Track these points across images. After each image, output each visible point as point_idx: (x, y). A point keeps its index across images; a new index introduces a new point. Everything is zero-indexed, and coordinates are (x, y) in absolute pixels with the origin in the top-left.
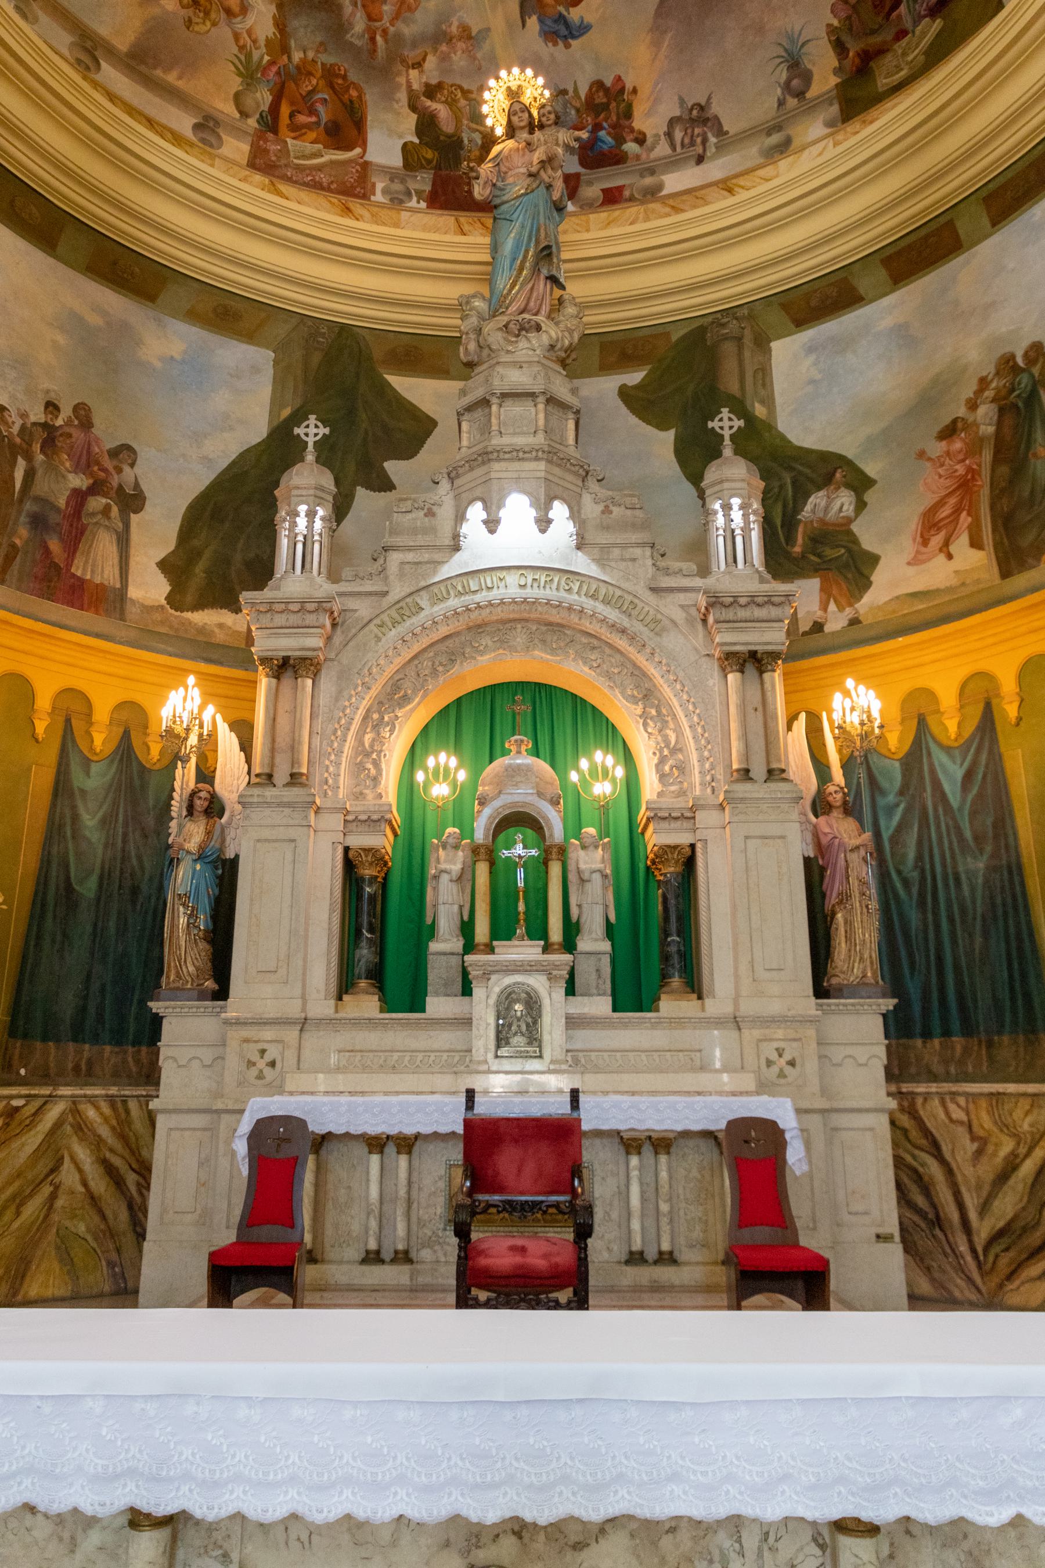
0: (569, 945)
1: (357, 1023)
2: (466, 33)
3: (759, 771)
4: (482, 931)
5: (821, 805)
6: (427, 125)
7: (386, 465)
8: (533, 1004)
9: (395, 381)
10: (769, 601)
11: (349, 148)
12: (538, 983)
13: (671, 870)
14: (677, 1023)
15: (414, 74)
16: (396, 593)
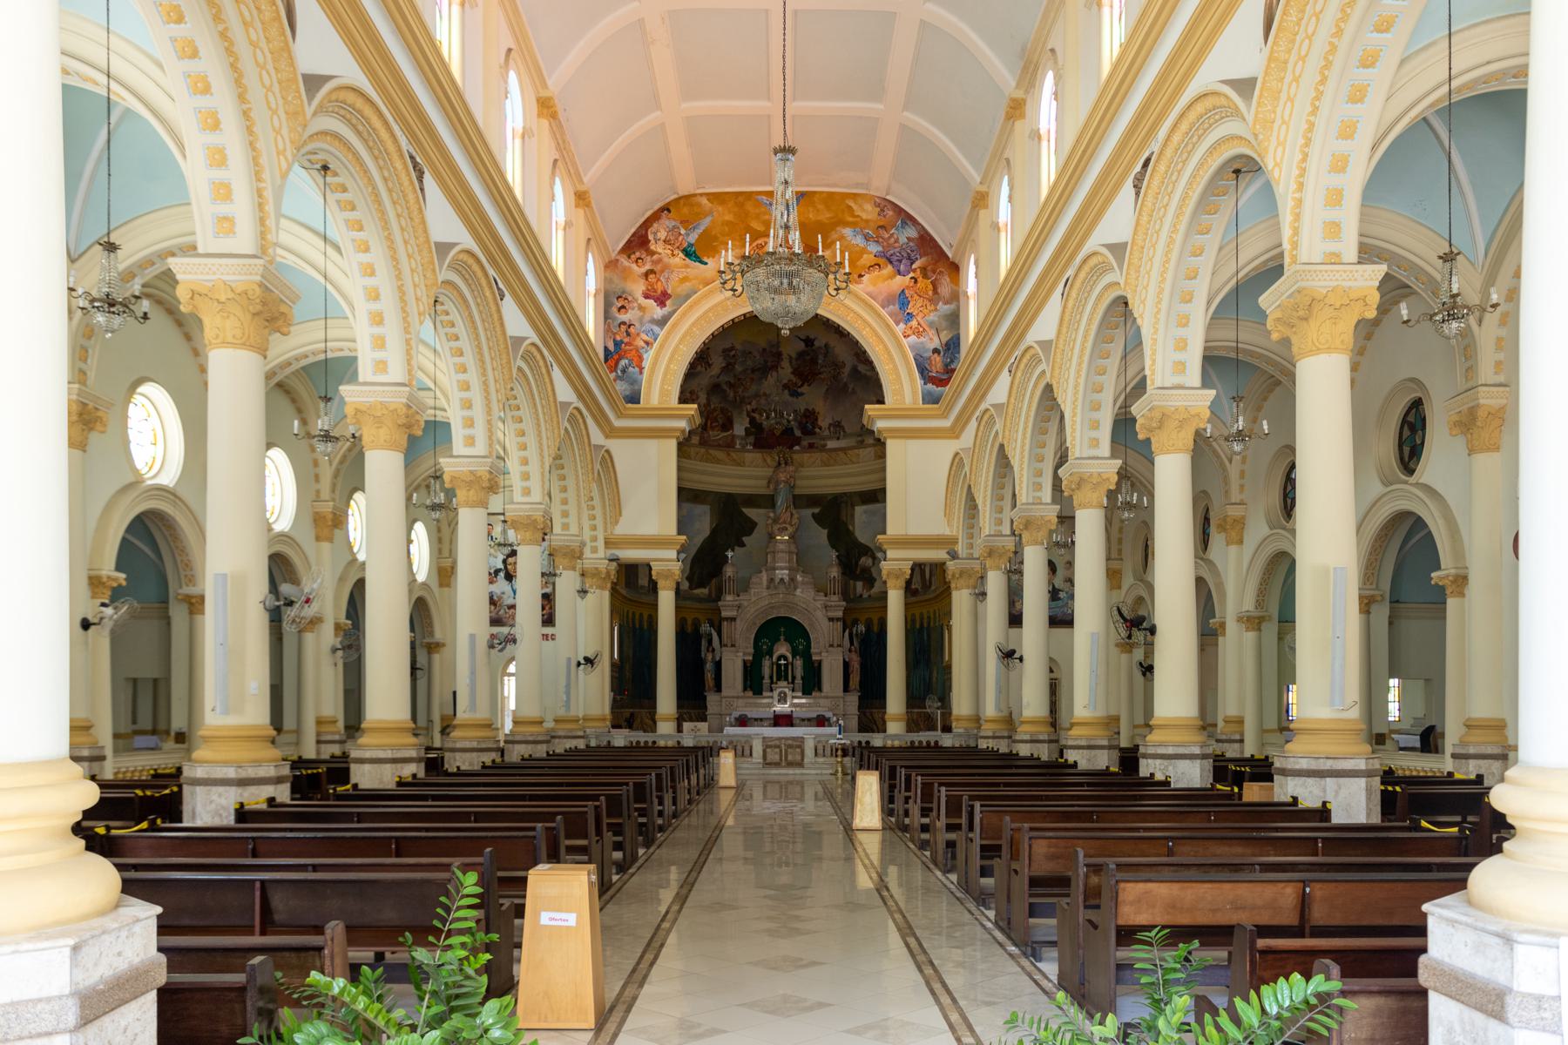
0: (793, 682)
1: (749, 697)
2: (765, 394)
3: (835, 645)
4: (775, 679)
5: (850, 651)
6: (752, 421)
7: (744, 539)
8: (785, 694)
9: (746, 511)
10: (839, 606)
11: (728, 430)
12: (786, 690)
13: (816, 665)
14: (815, 698)
15: (749, 407)
16: (753, 599)
